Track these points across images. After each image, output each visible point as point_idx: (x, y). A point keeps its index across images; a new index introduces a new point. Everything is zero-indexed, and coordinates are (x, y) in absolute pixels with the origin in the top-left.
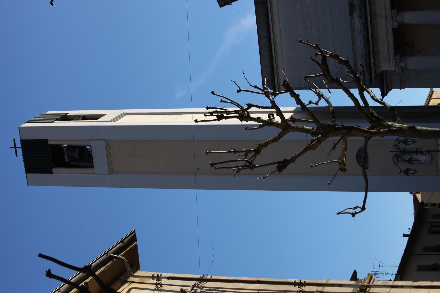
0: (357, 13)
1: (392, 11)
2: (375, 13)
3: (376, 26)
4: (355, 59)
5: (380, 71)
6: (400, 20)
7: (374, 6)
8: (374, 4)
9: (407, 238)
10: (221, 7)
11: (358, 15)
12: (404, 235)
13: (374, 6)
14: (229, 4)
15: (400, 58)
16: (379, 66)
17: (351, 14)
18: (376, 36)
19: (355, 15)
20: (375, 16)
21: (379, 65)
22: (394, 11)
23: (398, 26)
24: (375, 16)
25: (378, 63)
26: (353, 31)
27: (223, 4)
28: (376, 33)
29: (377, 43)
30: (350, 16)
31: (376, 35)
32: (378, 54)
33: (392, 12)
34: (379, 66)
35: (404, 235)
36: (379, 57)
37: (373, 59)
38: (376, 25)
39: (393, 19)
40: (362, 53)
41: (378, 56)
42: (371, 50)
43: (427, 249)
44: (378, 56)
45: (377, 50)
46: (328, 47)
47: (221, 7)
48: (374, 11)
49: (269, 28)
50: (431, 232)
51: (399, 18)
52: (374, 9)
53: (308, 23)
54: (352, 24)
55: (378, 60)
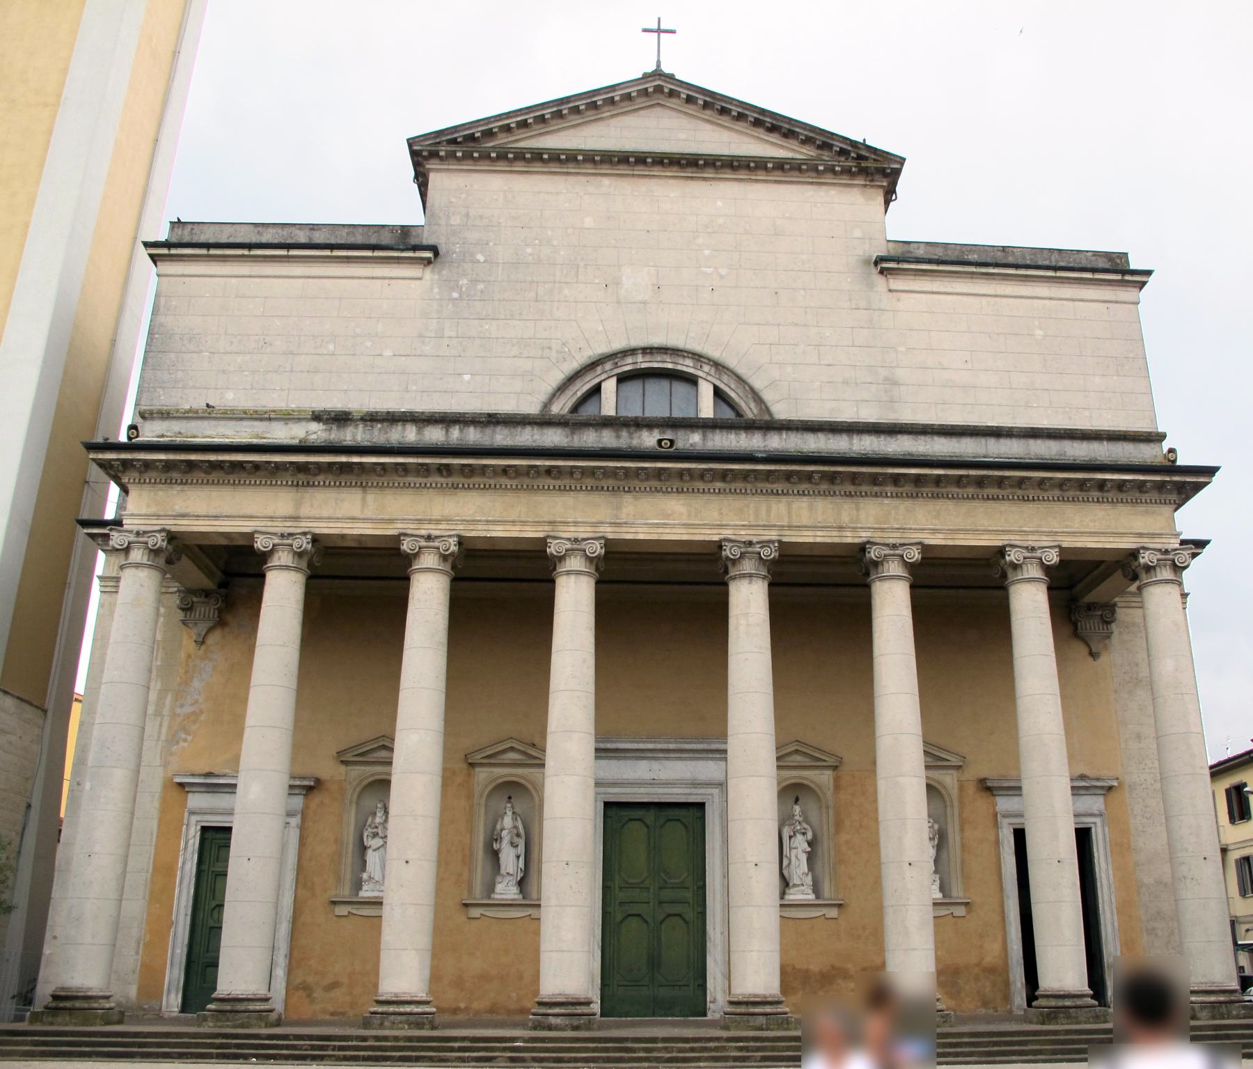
0: (319, 433)
1: (309, 537)
2: (311, 483)
3: (269, 482)
4: (178, 415)
5: (129, 486)
6: (279, 559)
7: (332, 483)
8: (338, 483)
10: (408, 140)
11: (314, 437)
13: (332, 483)
14: (416, 177)
15: (158, 545)
16: (142, 481)
17: (317, 417)
18: (237, 482)
19: (314, 426)
20: (300, 483)
21: (148, 481)
22: (308, 543)
23: (259, 549)
24: (300, 483)
25: (153, 481)
26: (266, 416)
27: (415, 148)
28: (247, 482)
29: (216, 482)
30: (313, 412)
31: (242, 482)
32: (182, 483)
33: (305, 534)
34: (142, 481)
36: (171, 483)
37: (167, 461)
38: (274, 482)
39: (282, 536)
40: (194, 437)
41: (174, 481)
42: (193, 457)
44: (174, 481)
45: (195, 481)
46: (255, 391)
47: (411, 143)
48: (316, 483)
49: (332, 247)
51: (283, 557)
52: (322, 483)
53: (331, 347)
54: (287, 417)
55: (163, 481)
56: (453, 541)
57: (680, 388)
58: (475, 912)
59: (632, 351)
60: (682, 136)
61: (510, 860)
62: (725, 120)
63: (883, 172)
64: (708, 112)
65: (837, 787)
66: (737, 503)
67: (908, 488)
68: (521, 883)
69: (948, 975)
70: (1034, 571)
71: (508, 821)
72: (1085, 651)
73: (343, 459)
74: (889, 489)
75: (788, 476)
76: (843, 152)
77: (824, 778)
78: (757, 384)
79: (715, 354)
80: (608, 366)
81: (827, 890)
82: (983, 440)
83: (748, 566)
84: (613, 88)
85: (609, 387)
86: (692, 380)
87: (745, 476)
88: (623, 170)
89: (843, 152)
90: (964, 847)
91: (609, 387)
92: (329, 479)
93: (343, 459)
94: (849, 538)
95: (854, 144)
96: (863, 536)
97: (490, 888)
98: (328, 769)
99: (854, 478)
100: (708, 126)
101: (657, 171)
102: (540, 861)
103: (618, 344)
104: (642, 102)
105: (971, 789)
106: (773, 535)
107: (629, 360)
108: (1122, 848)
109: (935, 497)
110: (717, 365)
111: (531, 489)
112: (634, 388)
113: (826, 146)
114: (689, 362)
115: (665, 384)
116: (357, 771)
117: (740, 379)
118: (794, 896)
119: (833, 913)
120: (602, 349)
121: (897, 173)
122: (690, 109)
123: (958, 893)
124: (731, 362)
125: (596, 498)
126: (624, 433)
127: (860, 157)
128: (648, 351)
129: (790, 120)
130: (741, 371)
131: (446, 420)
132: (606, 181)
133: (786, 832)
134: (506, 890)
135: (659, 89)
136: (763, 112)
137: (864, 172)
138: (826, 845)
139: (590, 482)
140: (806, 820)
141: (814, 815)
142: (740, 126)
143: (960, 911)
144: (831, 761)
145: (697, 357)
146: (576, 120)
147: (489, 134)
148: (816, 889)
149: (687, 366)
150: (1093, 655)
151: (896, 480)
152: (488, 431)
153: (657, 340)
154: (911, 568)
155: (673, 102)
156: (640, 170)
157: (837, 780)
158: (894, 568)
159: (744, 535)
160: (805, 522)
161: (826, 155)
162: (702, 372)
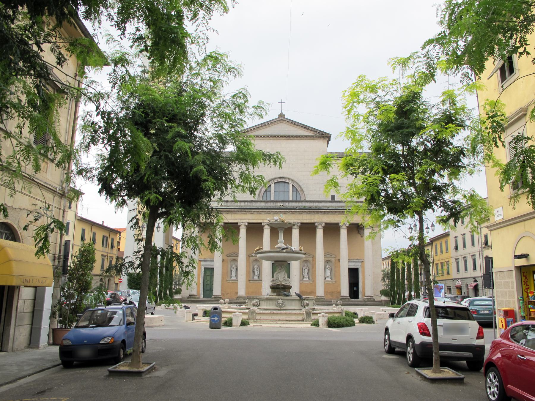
9: (101, 224)
12: (103, 222)
35: (103, 222)
43: (94, 234)
50: (104, 237)
56: (247, 223)
57: (286, 184)
58: (251, 282)
59: (277, 178)
60: (286, 129)
61: (256, 273)
62: (295, 126)
63: (327, 137)
64: (292, 124)
65: (313, 260)
66: (294, 215)
67: (323, 213)
68: (258, 277)
69: (326, 292)
70: (344, 227)
71: (256, 266)
72: (360, 236)
73: (228, 210)
74: (320, 213)
75: (302, 211)
76: (319, 133)
77: (311, 259)
78: (300, 184)
79: (292, 178)
80: (272, 181)
81: (311, 278)
82: (337, 203)
83: (295, 227)
84: (272, 120)
85: (273, 185)
86: (288, 183)
87: (295, 211)
88: (275, 138)
89: (319, 133)
90: (335, 271)
91: (273, 185)
92: (226, 213)
93: (228, 210)
94: (313, 222)
95: (321, 131)
96: (315, 221)
97: (253, 278)
98: (226, 258)
99: (313, 212)
100: (292, 127)
101: (281, 138)
102: (262, 275)
103: (274, 177)
104: (278, 122)
105: (337, 261)
106: (300, 221)
107: (276, 180)
108: (363, 272)
109: (328, 214)
110: (293, 181)
111: (259, 214)
112: (277, 185)
113: (315, 131)
114: (288, 180)
115: (283, 184)
116: (230, 258)
117: (297, 183)
118: (305, 279)
119: (312, 282)
120: (271, 178)
121: (330, 137)
122: (288, 123)
123: (333, 279)
124: (296, 180)
125: (270, 215)
126: (275, 203)
127: (322, 134)
128: (280, 178)
129: (308, 126)
130: (297, 181)
131: (245, 201)
132: (271, 141)
133: (304, 268)
134: (256, 278)
135: (282, 119)
136: (303, 125)
137: (323, 137)
138: (310, 271)
139: (269, 213)
140: (308, 266)
141: (309, 266)
142: (298, 127)
143: (334, 282)
144: (312, 256)
145: (289, 179)
146: (265, 127)
147: (248, 131)
148: (309, 278)
149: (287, 181)
150: (362, 237)
151: (321, 212)
152: (252, 203)
153: (281, 176)
154: (324, 227)
155: (284, 122)
156: (278, 138)
157: (313, 259)
158: (320, 227)
159: (295, 221)
160: (305, 219)
161: (316, 133)
162: (290, 182)
